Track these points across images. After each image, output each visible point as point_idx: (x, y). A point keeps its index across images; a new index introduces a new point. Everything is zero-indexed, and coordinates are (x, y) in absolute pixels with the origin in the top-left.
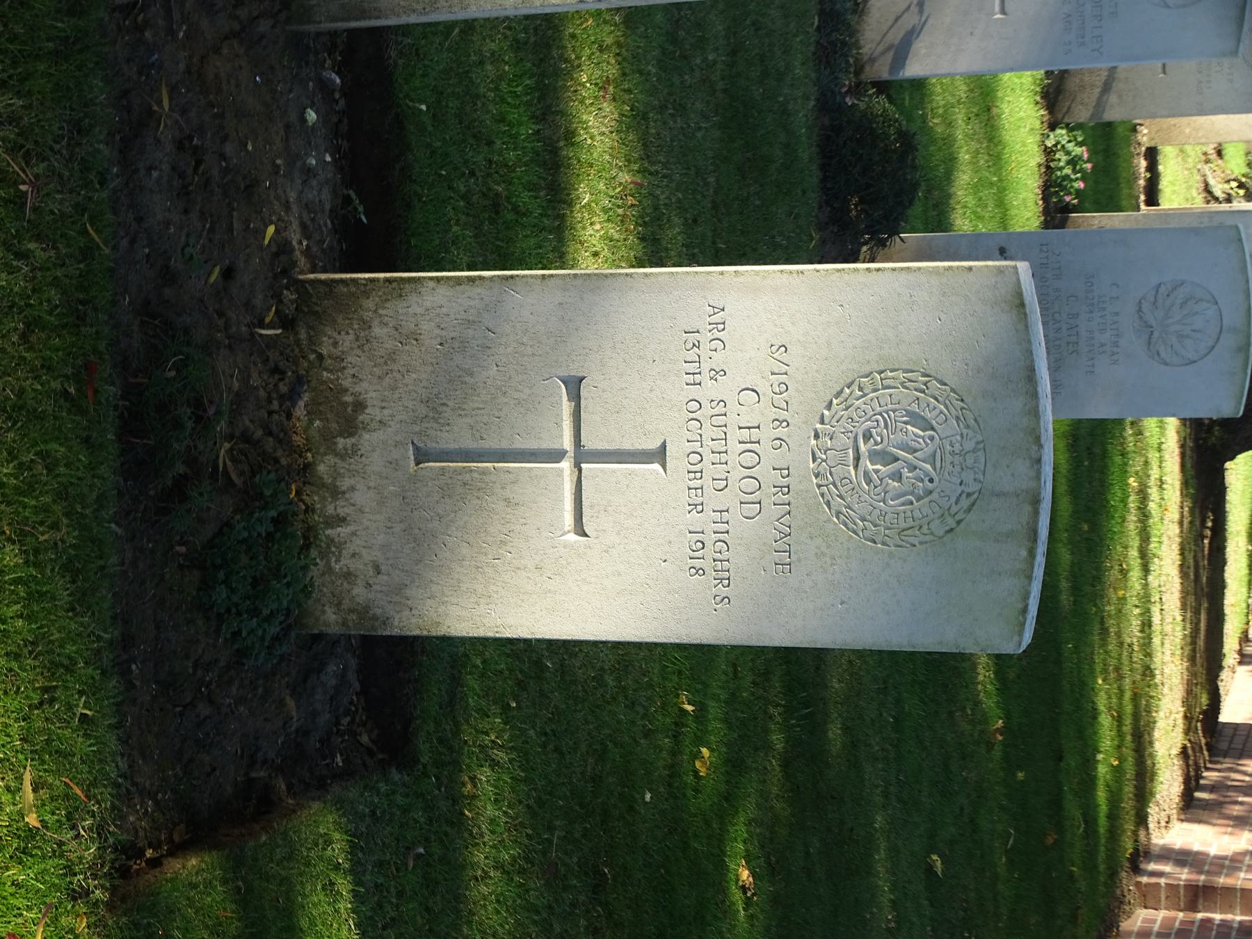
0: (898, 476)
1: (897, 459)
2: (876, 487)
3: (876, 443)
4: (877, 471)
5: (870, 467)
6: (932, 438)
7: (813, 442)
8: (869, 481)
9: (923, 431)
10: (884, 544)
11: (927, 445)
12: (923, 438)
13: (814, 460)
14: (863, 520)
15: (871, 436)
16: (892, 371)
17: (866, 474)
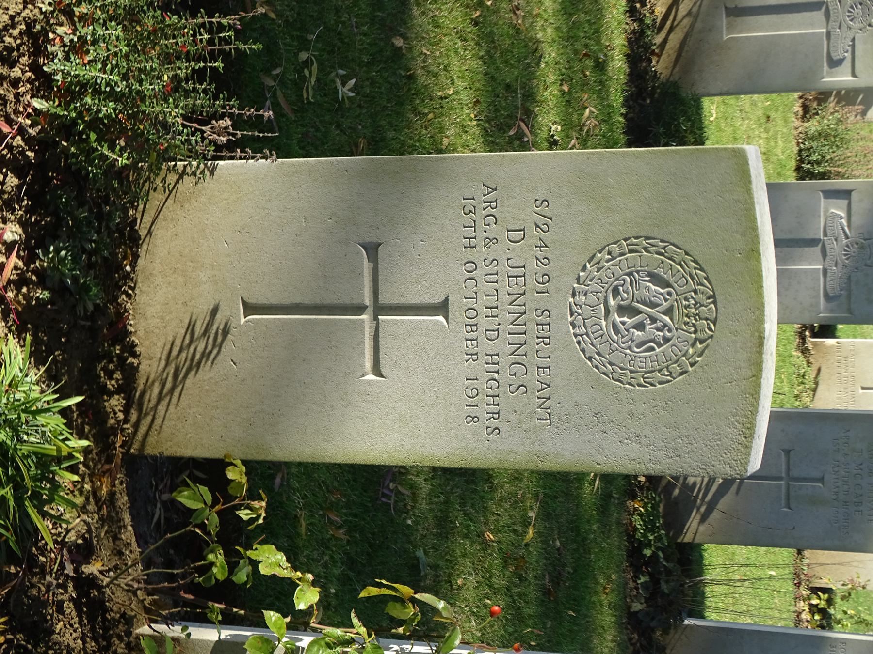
0: (640, 326)
1: (640, 312)
2: (623, 337)
3: (623, 300)
4: (623, 323)
5: (618, 319)
6: (669, 294)
7: (571, 300)
8: (617, 331)
9: (663, 289)
10: (630, 384)
11: (666, 300)
12: (662, 294)
13: (572, 315)
14: (611, 364)
15: (619, 293)
16: (636, 238)
17: (614, 326)
